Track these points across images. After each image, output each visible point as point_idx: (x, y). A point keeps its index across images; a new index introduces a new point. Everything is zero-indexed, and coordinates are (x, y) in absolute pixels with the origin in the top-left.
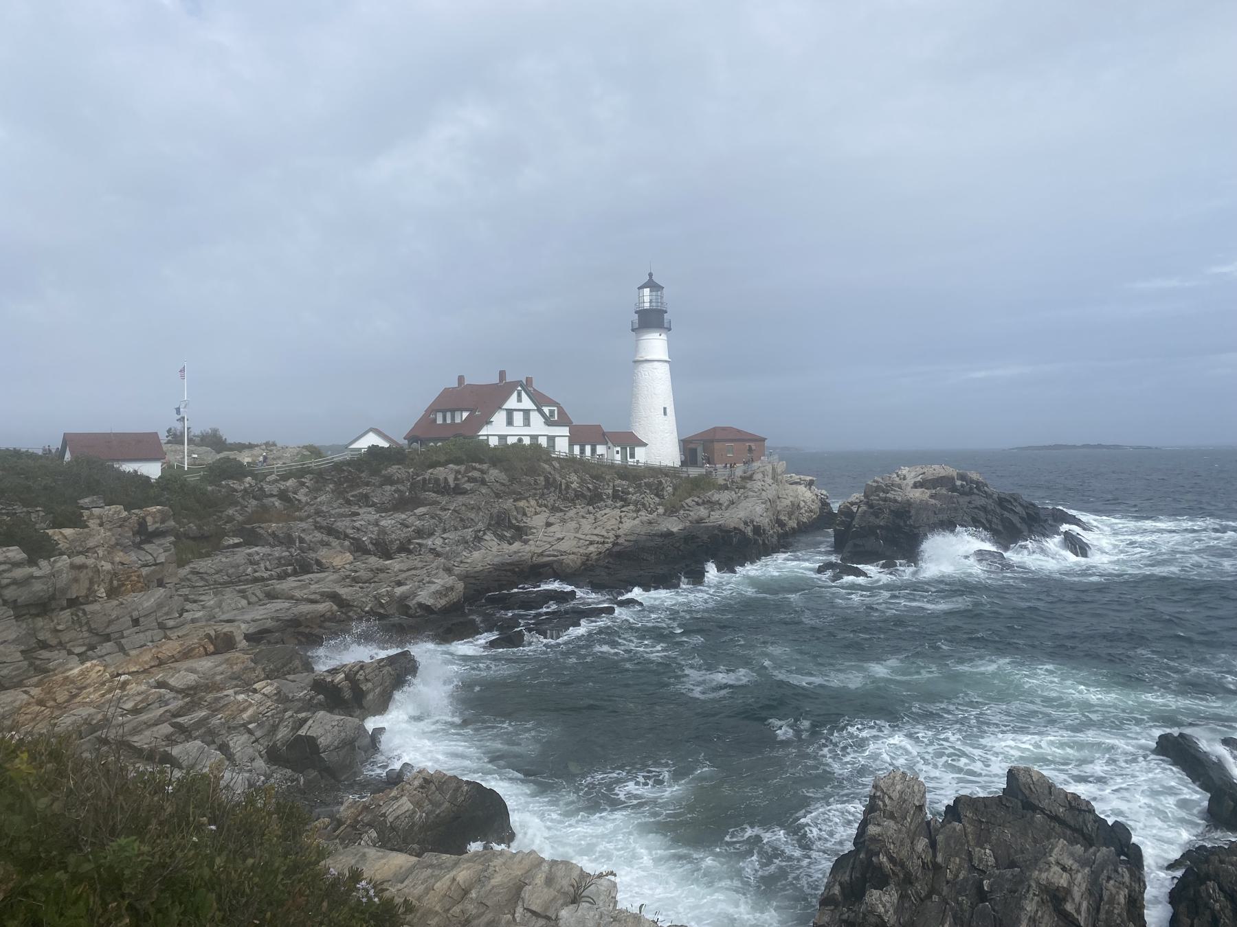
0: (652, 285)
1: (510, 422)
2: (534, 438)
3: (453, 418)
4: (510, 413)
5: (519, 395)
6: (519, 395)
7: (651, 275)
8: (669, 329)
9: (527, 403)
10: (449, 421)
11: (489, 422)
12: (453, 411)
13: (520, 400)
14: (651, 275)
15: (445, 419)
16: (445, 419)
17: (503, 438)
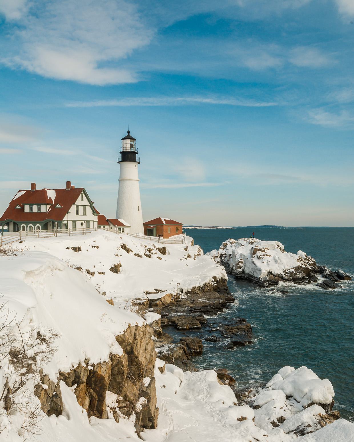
0: (128, 137)
1: (77, 213)
2: (88, 222)
3: (39, 209)
4: (78, 206)
5: (82, 196)
6: (82, 196)
7: (129, 132)
8: (139, 163)
9: (86, 202)
10: (35, 209)
11: (67, 212)
12: (39, 206)
13: (82, 200)
14: (129, 132)
15: (31, 209)
16: (31, 209)
17: (74, 222)
